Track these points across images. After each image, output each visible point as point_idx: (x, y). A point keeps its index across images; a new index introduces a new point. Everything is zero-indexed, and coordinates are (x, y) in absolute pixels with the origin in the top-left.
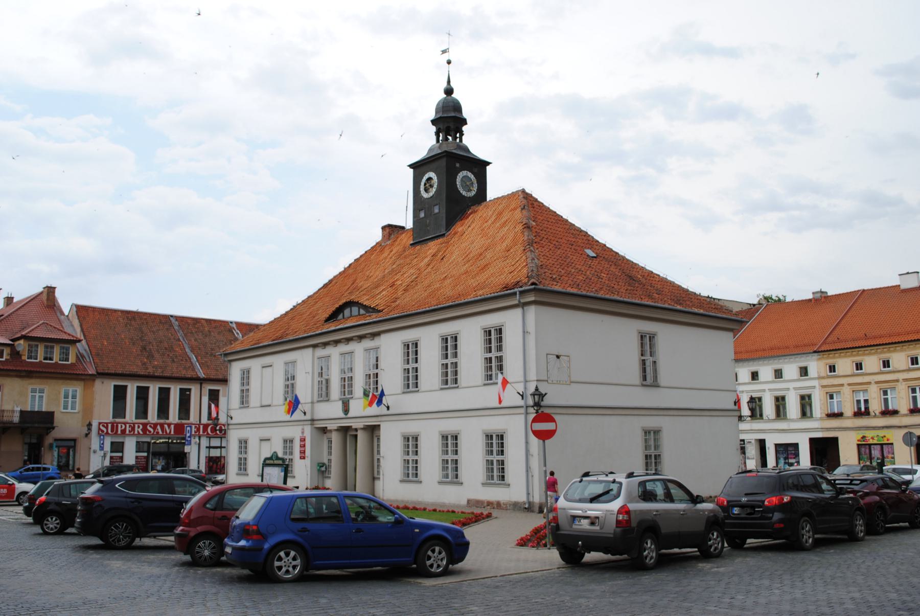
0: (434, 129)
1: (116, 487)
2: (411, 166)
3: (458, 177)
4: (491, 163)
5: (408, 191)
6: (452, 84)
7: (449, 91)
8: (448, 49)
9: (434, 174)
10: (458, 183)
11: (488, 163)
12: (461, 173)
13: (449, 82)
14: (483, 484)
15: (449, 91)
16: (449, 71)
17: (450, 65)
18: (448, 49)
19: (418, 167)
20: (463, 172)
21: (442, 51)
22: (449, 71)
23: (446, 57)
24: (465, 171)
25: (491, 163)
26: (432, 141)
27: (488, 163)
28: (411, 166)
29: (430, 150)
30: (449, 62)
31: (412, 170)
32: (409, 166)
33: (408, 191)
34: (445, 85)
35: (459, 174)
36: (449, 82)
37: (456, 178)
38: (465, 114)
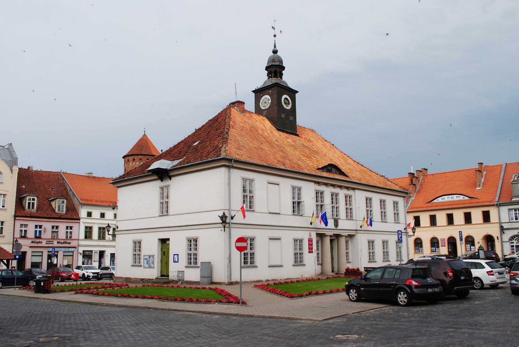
2: (253, 91)
3: (282, 98)
4: (298, 92)
7: (275, 52)
9: (268, 96)
10: (282, 101)
11: (297, 92)
12: (284, 96)
13: (275, 47)
14: (293, 265)
15: (275, 52)
17: (276, 37)
19: (259, 93)
20: (285, 95)
24: (286, 95)
25: (298, 92)
27: (297, 92)
29: (265, 83)
32: (252, 91)
34: (272, 48)
35: (283, 97)
36: (275, 47)
37: (282, 99)
38: (284, 65)
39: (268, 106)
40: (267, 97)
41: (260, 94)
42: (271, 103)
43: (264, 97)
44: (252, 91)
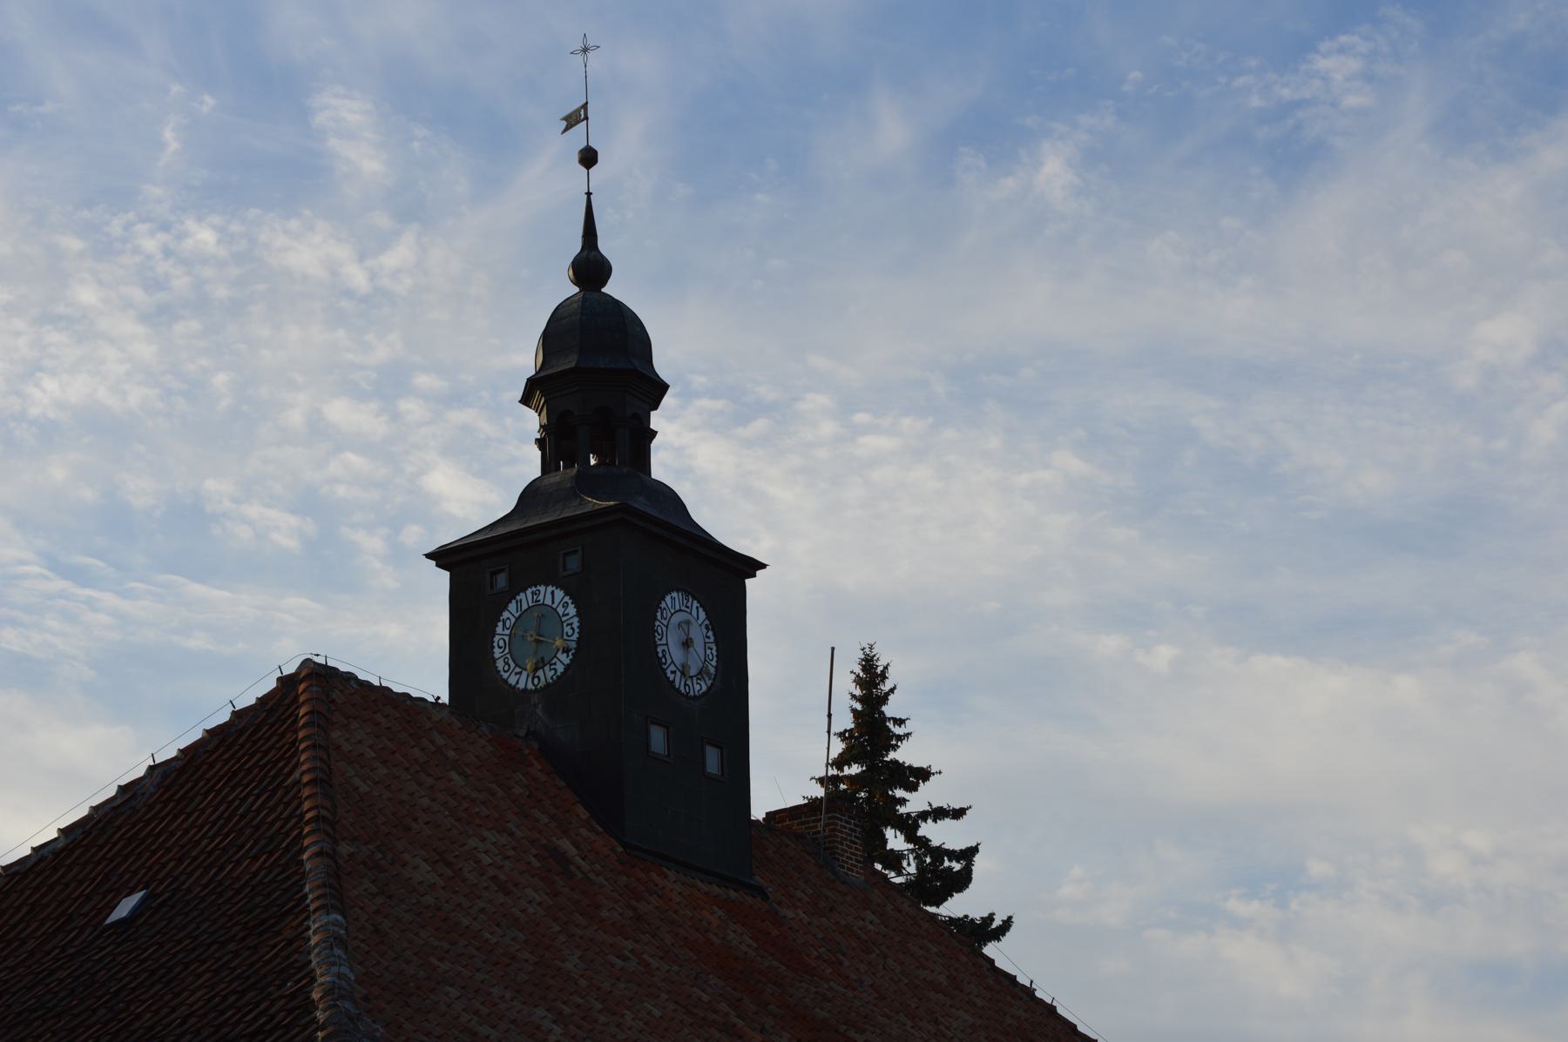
0: (531, 421)
1: (917, 868)
2: (441, 557)
4: (763, 566)
5: (833, 649)
6: (605, 246)
8: (585, 106)
9: (559, 594)
11: (752, 566)
12: (668, 599)
16: (589, 194)
18: (585, 106)
20: (675, 594)
21: (566, 119)
22: (589, 194)
23: (577, 138)
25: (763, 566)
26: (529, 466)
27: (752, 566)
28: (441, 557)
29: (530, 497)
30: (589, 158)
31: (446, 574)
33: (833, 649)
34: (576, 247)
39: (560, 669)
40: (553, 596)
41: (494, 574)
42: (579, 641)
43: (526, 598)
44: (429, 556)
